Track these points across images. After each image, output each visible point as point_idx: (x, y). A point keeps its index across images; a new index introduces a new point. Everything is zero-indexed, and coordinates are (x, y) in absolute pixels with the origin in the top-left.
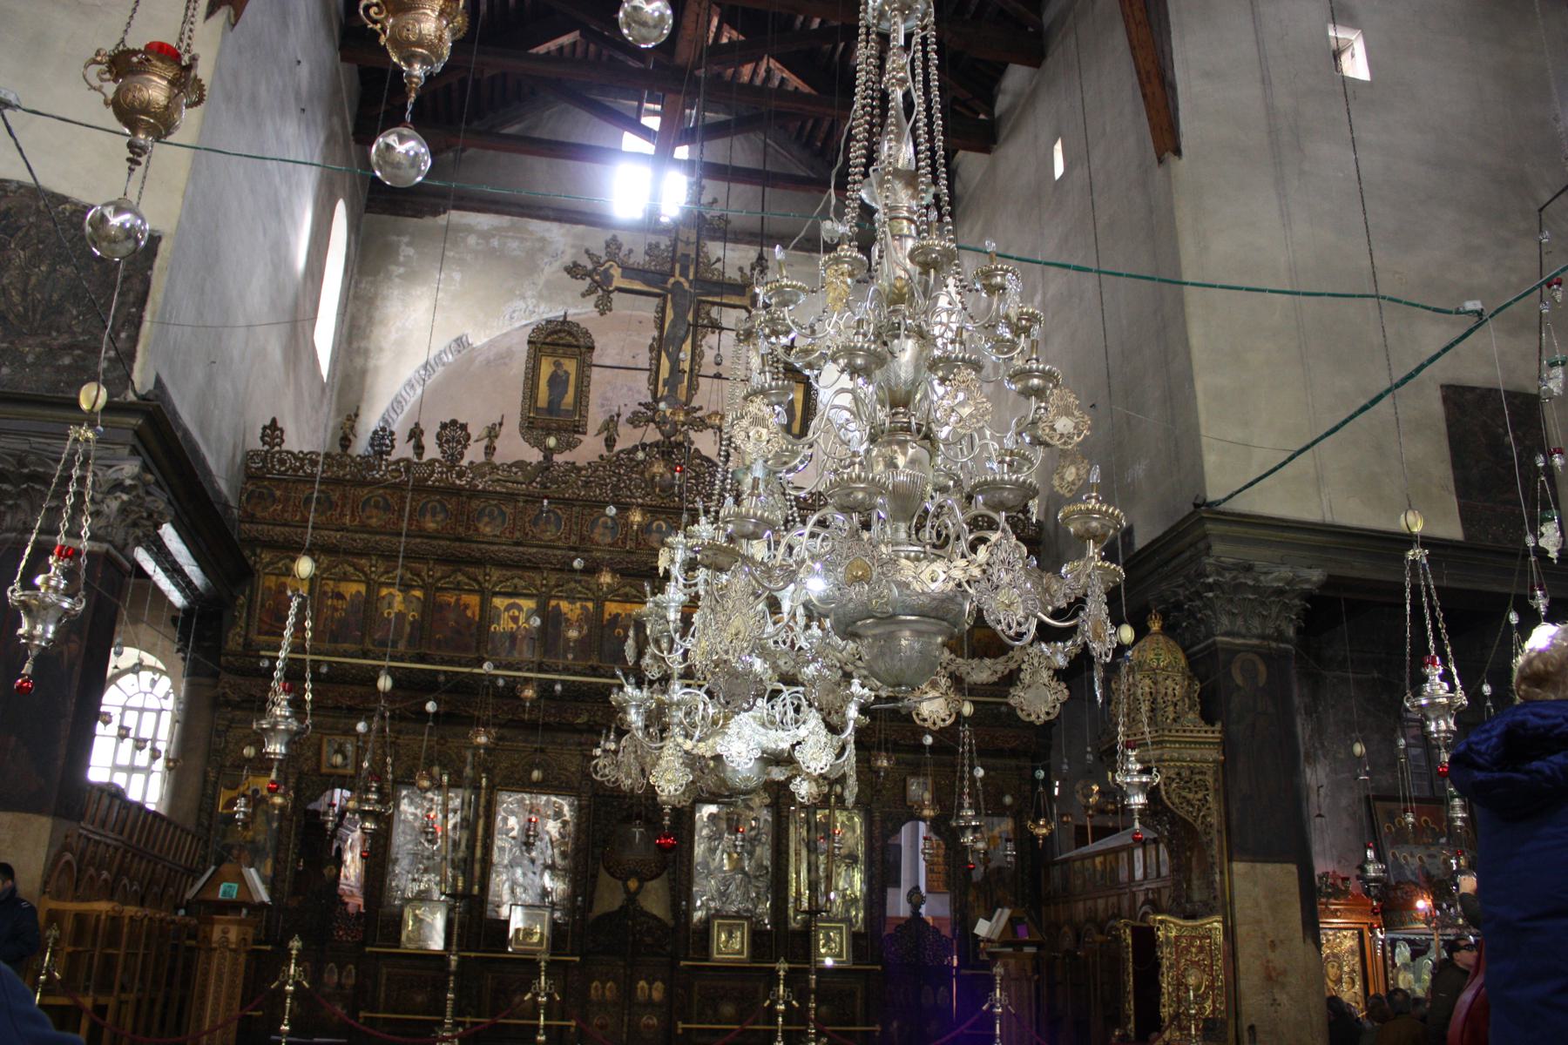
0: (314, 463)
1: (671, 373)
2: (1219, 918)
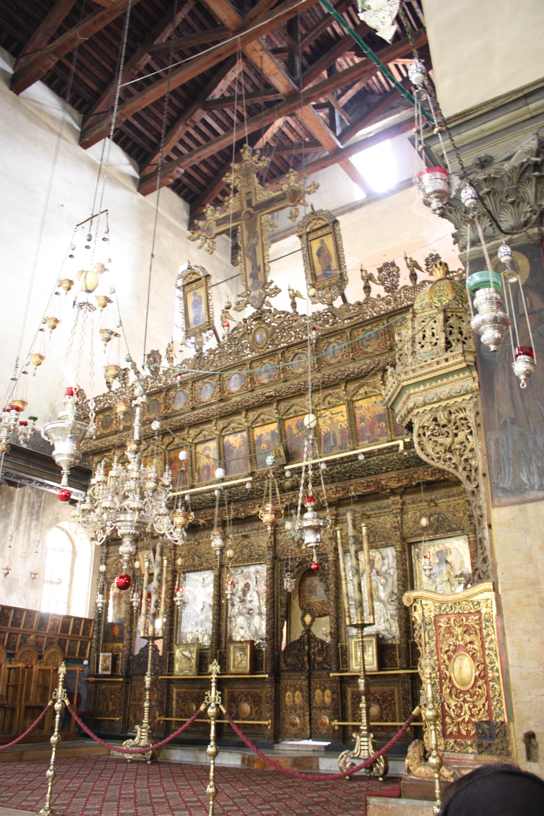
0: (100, 401)
1: (253, 268)
2: (488, 585)
